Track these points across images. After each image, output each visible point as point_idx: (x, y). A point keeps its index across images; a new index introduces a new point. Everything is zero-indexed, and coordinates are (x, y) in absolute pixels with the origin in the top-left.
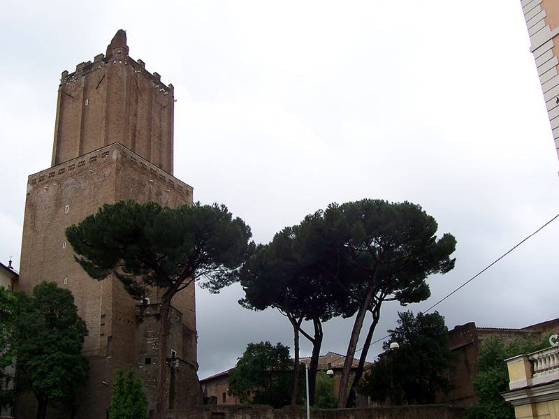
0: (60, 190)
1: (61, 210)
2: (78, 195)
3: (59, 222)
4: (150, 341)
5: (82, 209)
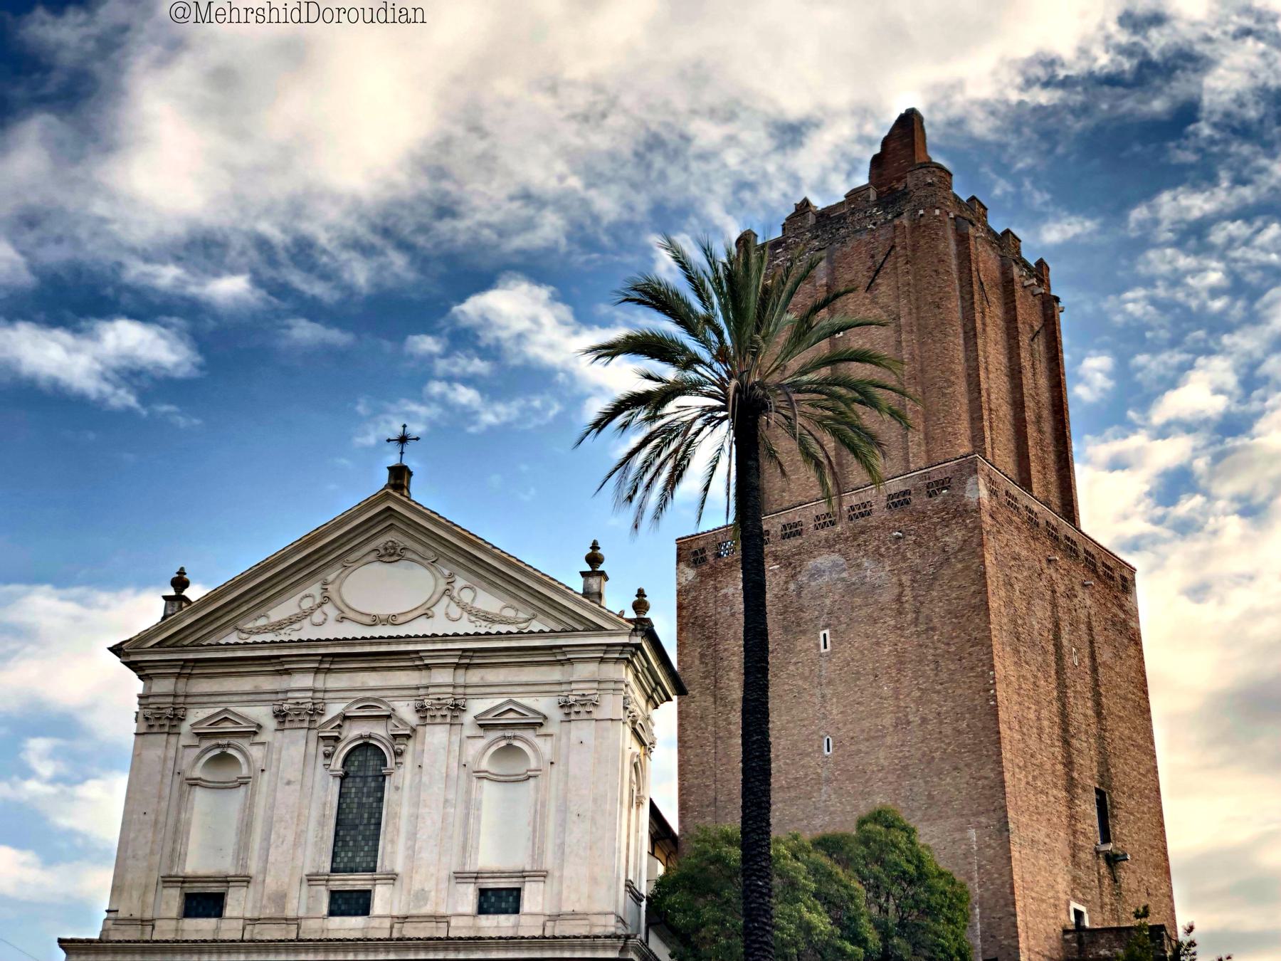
0: (792, 586)
2: (858, 601)
5: (878, 643)
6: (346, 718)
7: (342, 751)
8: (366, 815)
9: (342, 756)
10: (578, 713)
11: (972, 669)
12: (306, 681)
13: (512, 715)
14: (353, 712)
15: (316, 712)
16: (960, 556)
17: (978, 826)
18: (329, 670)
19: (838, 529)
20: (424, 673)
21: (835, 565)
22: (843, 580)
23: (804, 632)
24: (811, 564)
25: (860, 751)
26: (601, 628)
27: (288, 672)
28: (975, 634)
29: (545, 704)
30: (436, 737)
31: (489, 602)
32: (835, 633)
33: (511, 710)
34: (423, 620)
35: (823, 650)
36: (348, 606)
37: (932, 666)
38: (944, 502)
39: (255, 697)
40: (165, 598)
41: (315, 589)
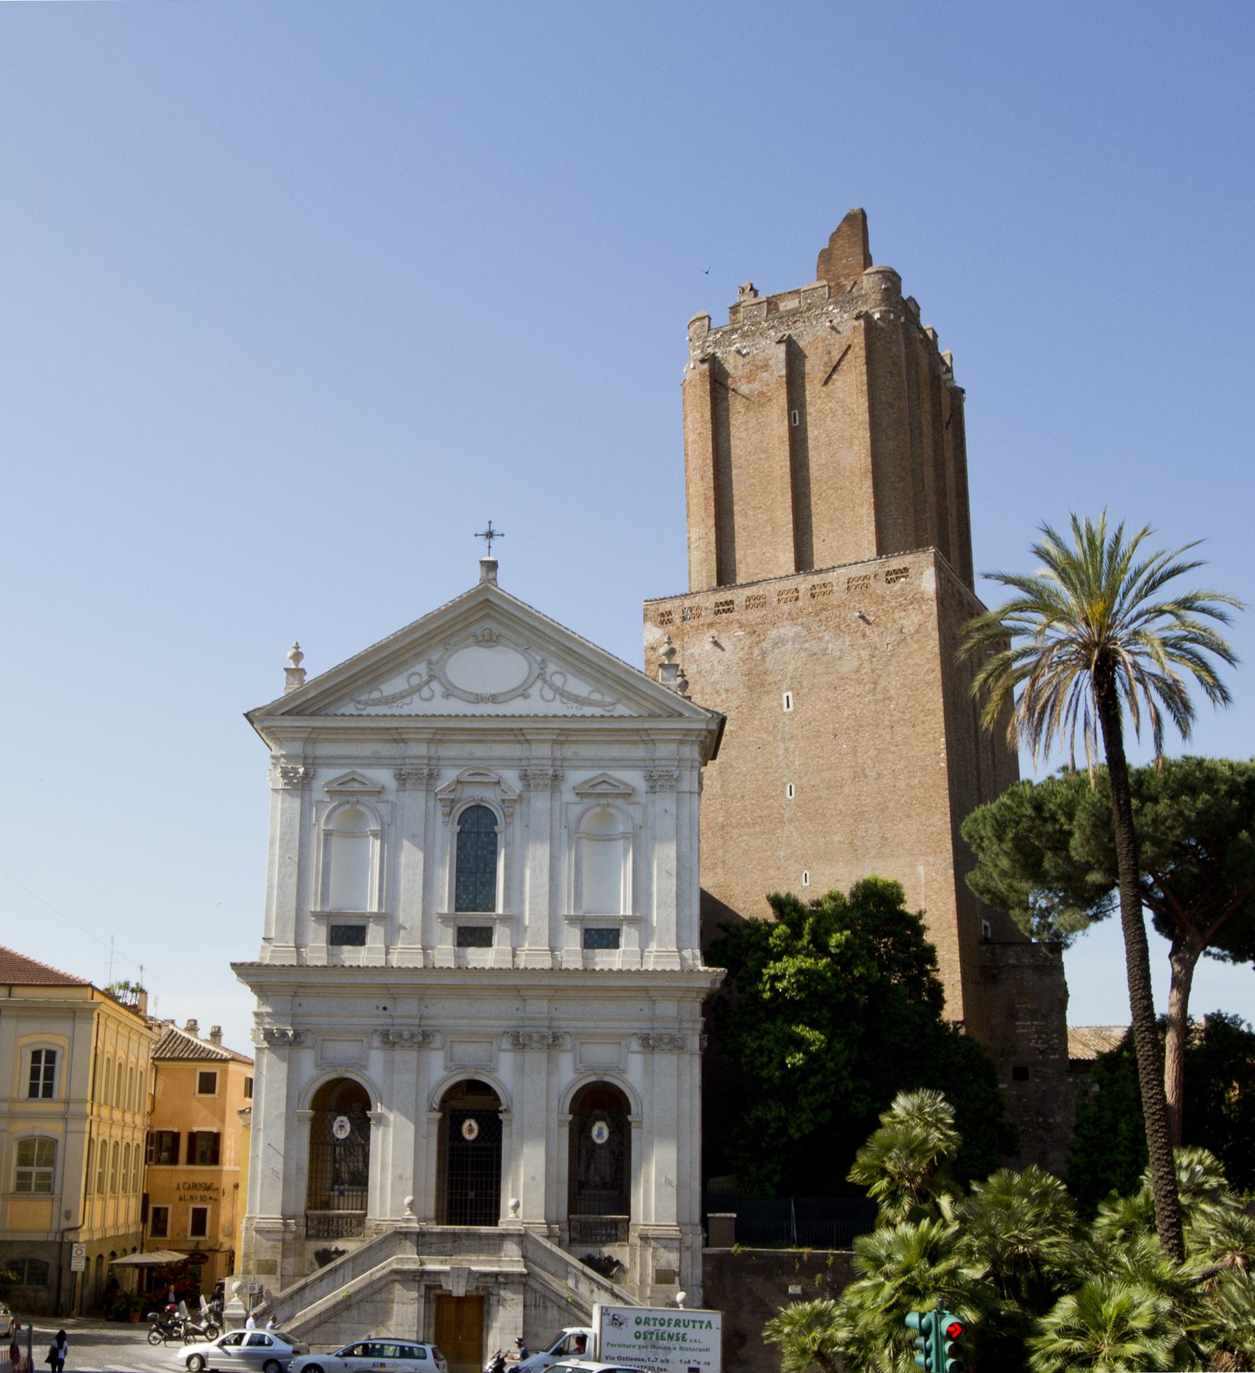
0: (756, 652)
1: (766, 702)
2: (819, 670)
3: (766, 730)
4: (1023, 1027)
6: (459, 782)
7: (459, 809)
13: (605, 786)
14: (465, 778)
15: (432, 777)
16: (916, 637)
17: (927, 864)
18: (441, 741)
19: (800, 604)
20: (525, 746)
21: (797, 635)
22: (806, 649)
23: (767, 693)
24: (773, 633)
25: (820, 798)
26: (681, 715)
27: (403, 741)
28: (928, 706)
30: (540, 803)
31: (578, 686)
32: (796, 695)
34: (520, 701)
35: (785, 709)
37: (889, 730)
38: (902, 589)
39: (376, 761)
40: (286, 670)
41: (422, 668)
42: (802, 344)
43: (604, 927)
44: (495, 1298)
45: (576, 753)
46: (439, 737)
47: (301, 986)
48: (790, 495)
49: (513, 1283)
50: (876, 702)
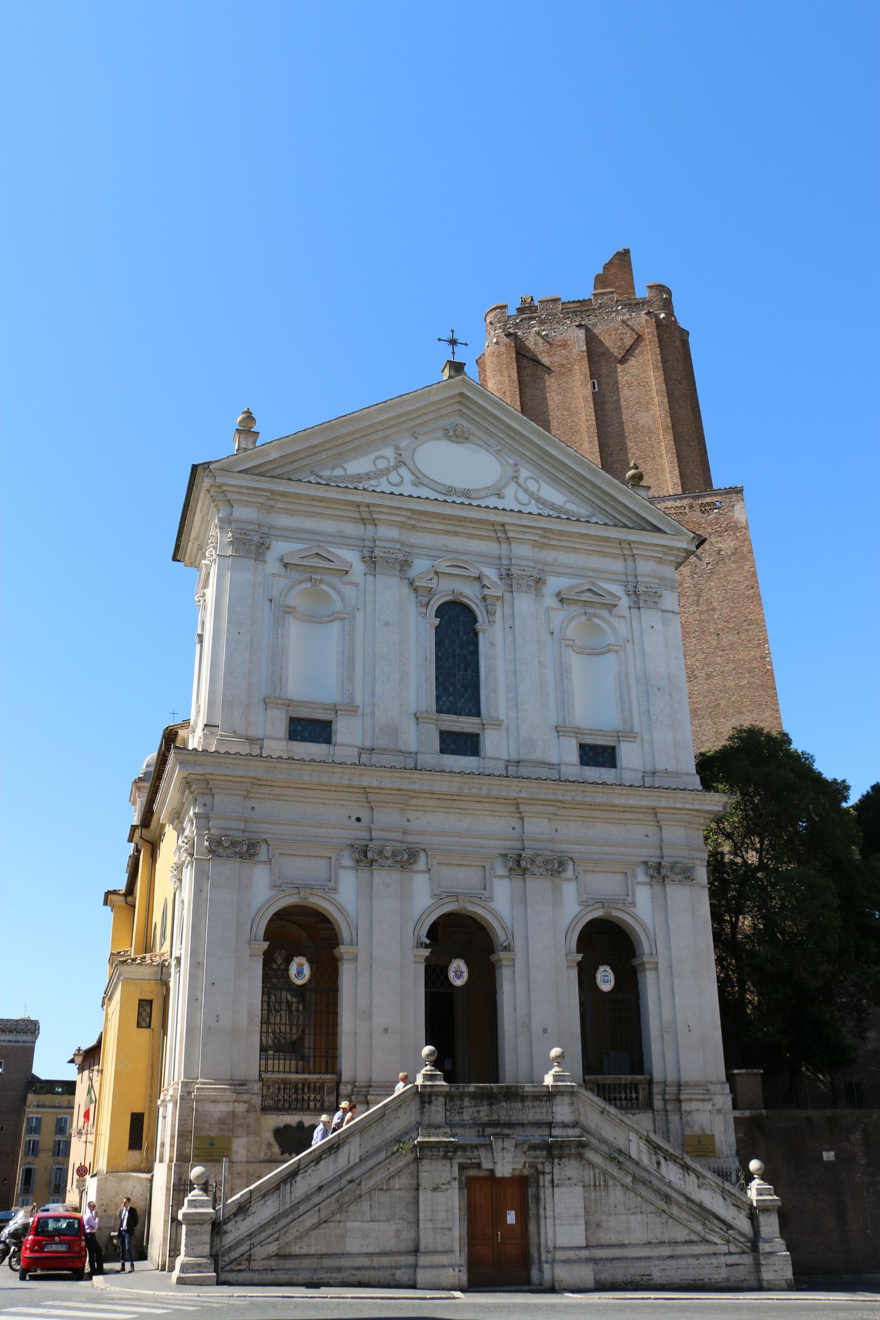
8: (462, 665)
9: (435, 608)
10: (646, 601)
11: (750, 641)
12: (393, 533)
29: (617, 589)
30: (524, 603)
33: (590, 590)
36: (424, 475)
42: (596, 331)
43: (599, 742)
44: (548, 1177)
45: (555, 559)
46: (413, 522)
47: (258, 782)
48: (597, 443)
49: (569, 1156)
50: (701, 613)
